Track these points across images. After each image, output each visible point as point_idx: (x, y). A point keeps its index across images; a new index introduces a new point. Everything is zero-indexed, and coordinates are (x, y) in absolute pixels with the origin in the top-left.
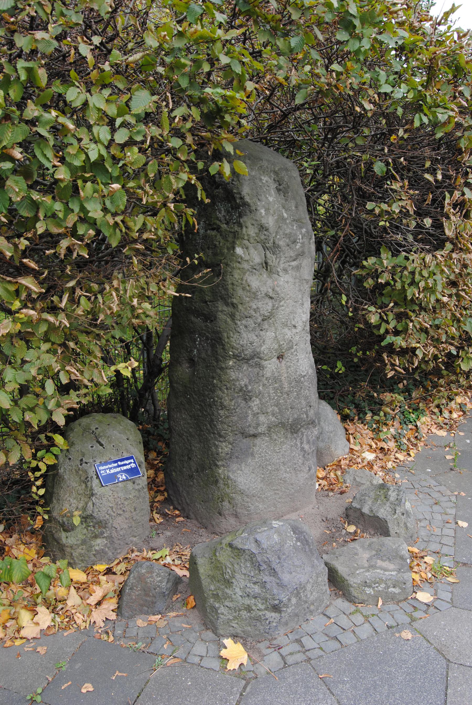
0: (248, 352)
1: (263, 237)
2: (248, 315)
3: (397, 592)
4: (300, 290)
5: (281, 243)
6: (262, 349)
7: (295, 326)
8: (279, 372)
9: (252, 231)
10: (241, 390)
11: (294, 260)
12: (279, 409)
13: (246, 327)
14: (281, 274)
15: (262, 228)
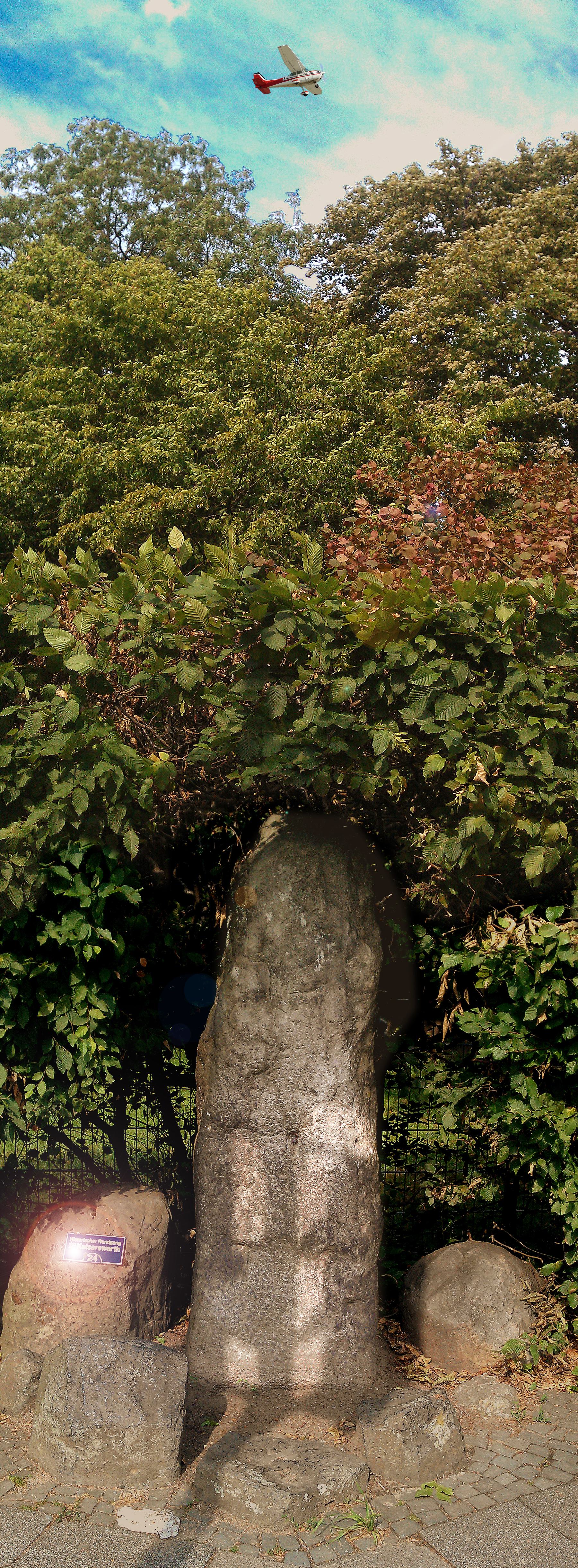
0: (229, 1115)
1: (267, 953)
2: (230, 1063)
3: (256, 1511)
4: (322, 1037)
5: (291, 963)
6: (253, 1115)
7: (314, 1092)
8: (287, 1157)
9: (251, 943)
10: (221, 1170)
11: (311, 990)
12: (285, 1213)
13: (227, 1079)
14: (285, 1008)
15: (264, 940)
